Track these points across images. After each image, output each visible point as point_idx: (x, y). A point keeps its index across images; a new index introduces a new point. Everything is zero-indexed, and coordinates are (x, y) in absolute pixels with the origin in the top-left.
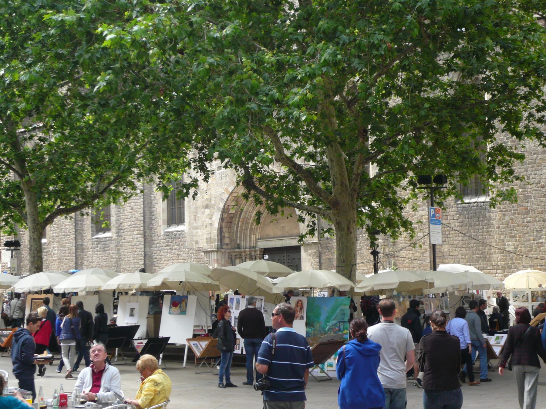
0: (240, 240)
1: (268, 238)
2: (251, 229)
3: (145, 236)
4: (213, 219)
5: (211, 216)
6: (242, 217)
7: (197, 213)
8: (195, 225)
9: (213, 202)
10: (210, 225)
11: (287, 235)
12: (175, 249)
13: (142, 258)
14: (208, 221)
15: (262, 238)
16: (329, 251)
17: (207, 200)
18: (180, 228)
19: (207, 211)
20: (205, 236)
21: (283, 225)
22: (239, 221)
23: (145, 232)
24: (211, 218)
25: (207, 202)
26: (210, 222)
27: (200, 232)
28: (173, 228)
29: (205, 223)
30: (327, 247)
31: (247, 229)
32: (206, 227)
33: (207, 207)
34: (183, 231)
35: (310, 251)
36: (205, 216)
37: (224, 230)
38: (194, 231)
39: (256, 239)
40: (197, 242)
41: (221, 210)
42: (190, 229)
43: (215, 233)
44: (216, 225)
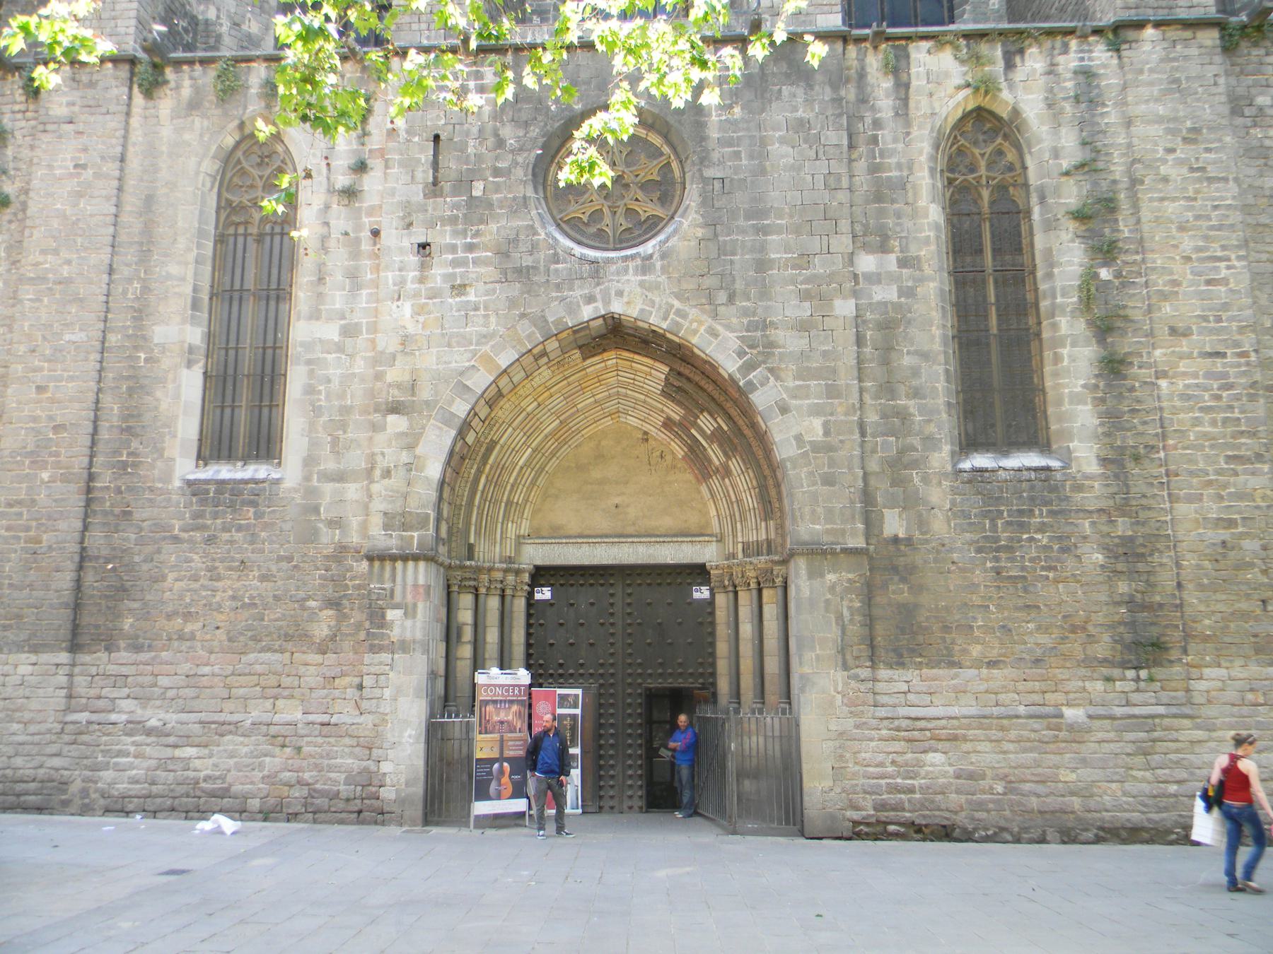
0: (478, 533)
1: (557, 534)
2: (509, 503)
3: (89, 490)
4: (419, 450)
5: (410, 441)
6: (491, 461)
7: (343, 426)
8: (330, 465)
9: (425, 394)
10: (402, 472)
11: (630, 530)
12: (232, 542)
13: (71, 565)
14: (392, 455)
15: (536, 535)
16: (903, 580)
17: (399, 386)
18: (259, 471)
19: (396, 423)
20: (378, 505)
21: (617, 500)
22: (479, 472)
23: (91, 477)
24: (410, 447)
25: (396, 392)
26: (405, 457)
27: (353, 491)
28: (224, 471)
29: (382, 463)
30: (895, 569)
31: (496, 502)
32: (387, 473)
33: (395, 408)
34: (277, 482)
35: (831, 577)
36: (380, 438)
37: (447, 490)
38: (328, 488)
39: (518, 537)
40: (336, 523)
41: (458, 423)
42: (307, 478)
43: (424, 495)
44: (434, 469)
